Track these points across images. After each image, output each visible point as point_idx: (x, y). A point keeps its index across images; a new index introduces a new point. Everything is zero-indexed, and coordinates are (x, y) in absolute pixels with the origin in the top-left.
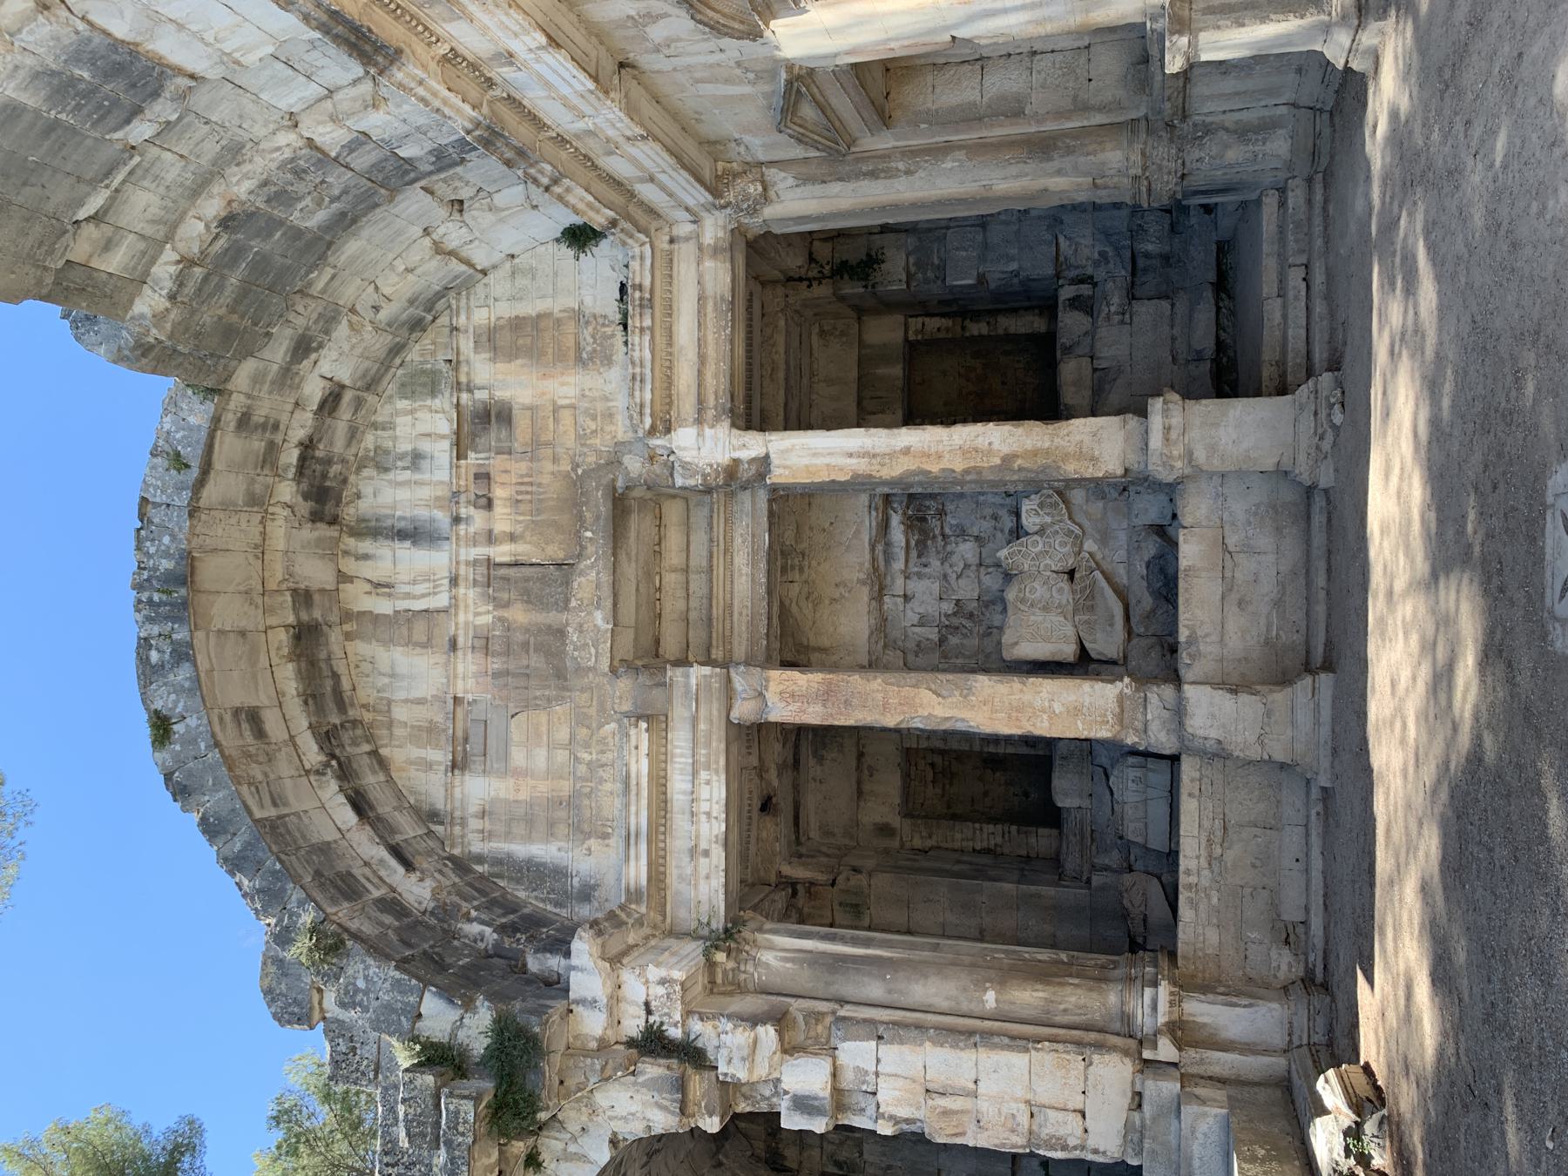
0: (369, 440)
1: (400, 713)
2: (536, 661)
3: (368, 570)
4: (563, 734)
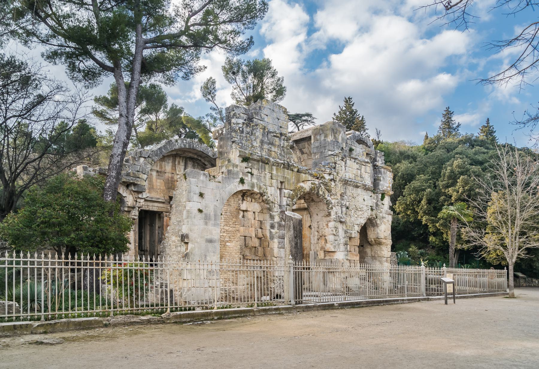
0: (196, 164)
1: (163, 163)
2: (170, 185)
3: (181, 161)
4: (161, 188)
